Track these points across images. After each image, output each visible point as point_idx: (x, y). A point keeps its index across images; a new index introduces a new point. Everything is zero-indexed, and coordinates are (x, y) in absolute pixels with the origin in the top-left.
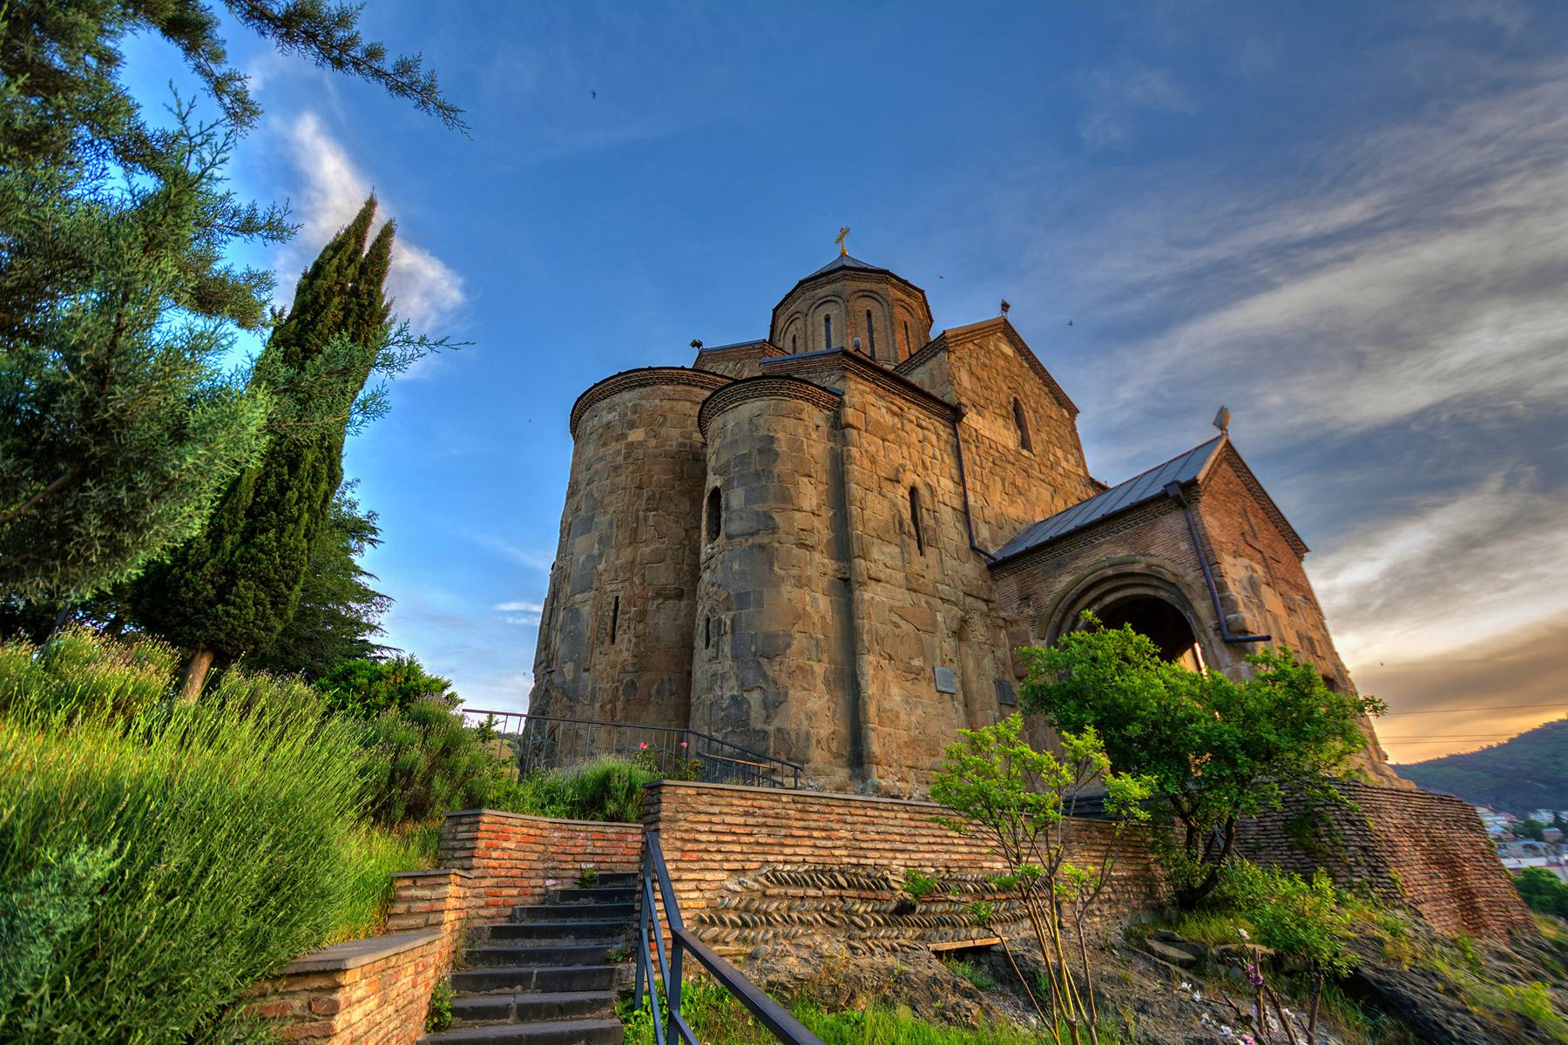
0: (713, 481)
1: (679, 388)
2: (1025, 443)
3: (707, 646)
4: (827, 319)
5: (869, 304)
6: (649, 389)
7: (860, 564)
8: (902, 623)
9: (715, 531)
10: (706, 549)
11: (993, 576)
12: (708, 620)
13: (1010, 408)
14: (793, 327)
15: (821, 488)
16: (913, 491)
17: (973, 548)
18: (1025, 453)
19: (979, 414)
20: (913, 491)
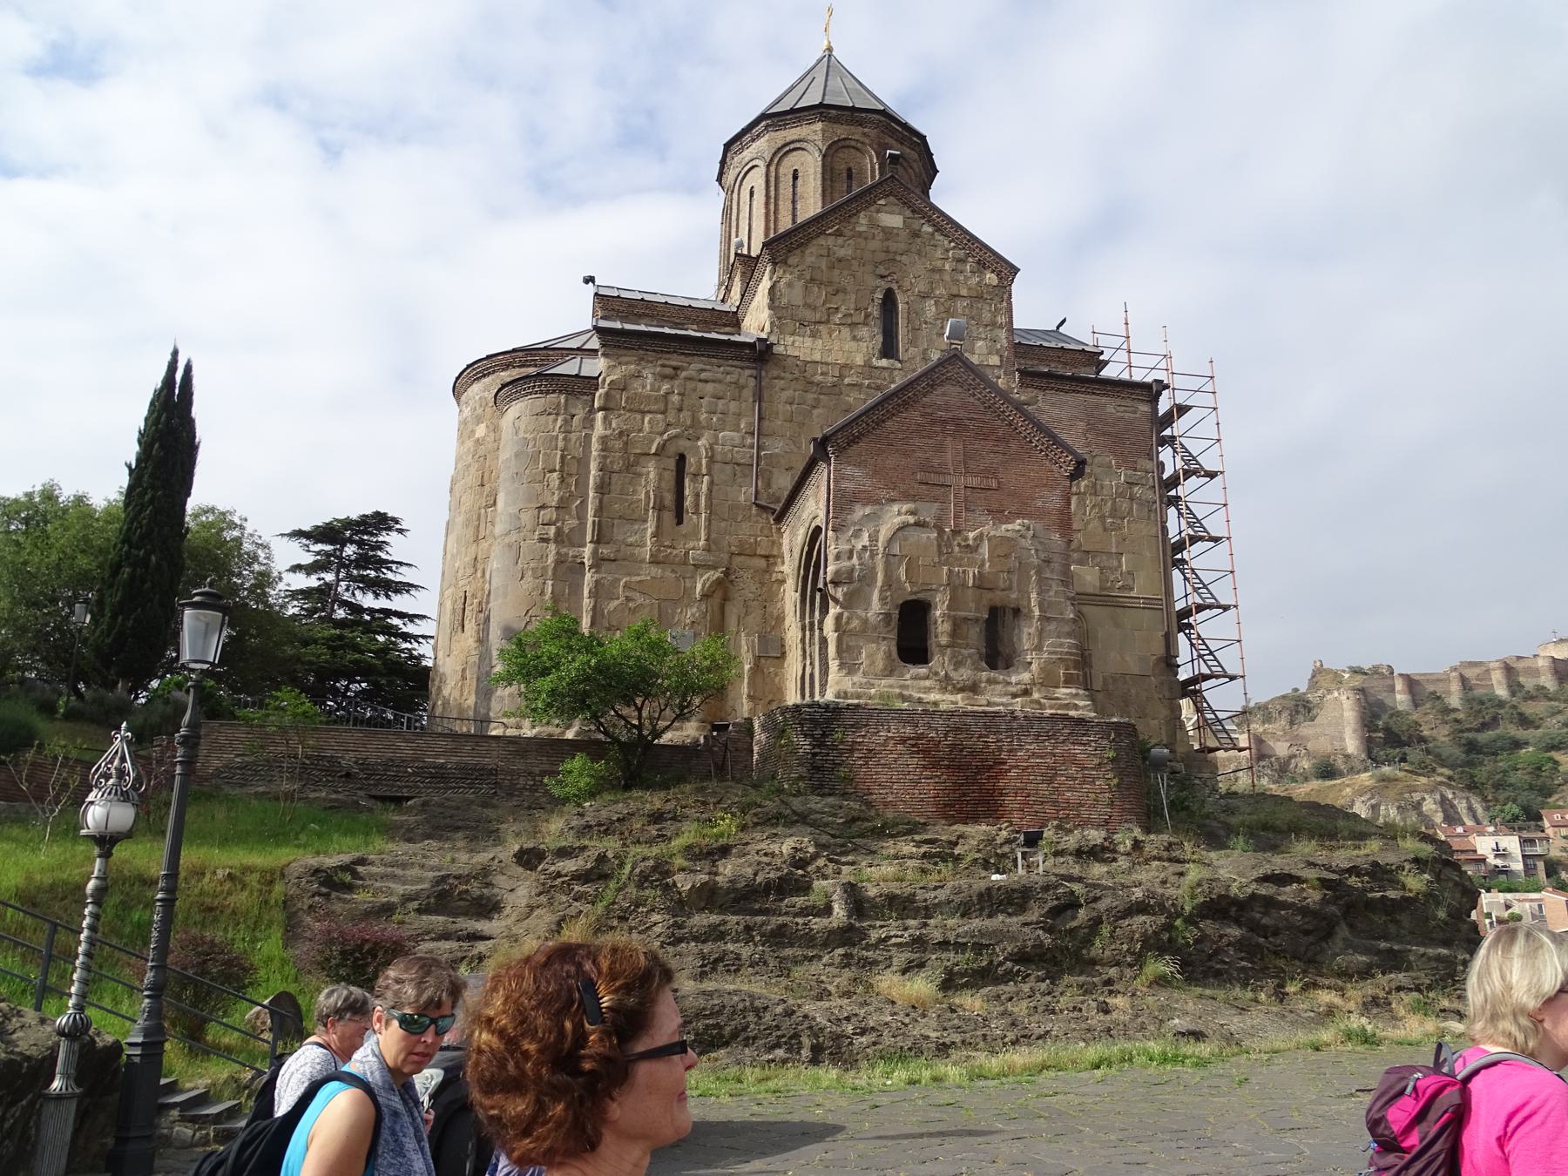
13: (875, 311)
18: (884, 362)
19: (814, 335)
20: (681, 459)
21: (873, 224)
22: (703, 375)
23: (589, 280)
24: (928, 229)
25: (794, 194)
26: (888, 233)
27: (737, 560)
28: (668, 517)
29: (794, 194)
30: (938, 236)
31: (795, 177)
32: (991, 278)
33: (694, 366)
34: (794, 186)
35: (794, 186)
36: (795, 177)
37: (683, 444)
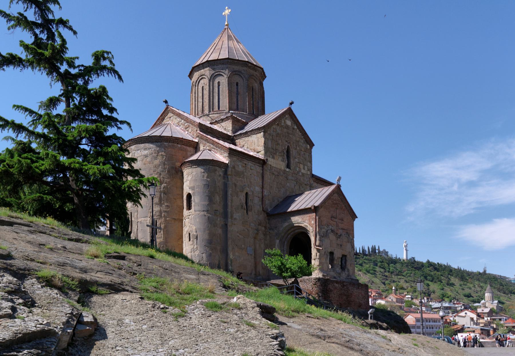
0: (187, 189)
1: (170, 144)
2: (288, 166)
3: (190, 240)
4: (219, 86)
5: (237, 79)
6: (159, 143)
7: (229, 220)
8: (240, 236)
9: (189, 207)
10: (186, 212)
11: (269, 220)
12: (190, 234)
13: (285, 152)
14: (202, 81)
15: (220, 196)
16: (247, 194)
17: (263, 210)
18: (288, 170)
19: (273, 158)
20: (247, 194)
21: (285, 122)
22: (252, 168)
23: (166, 102)
24: (296, 127)
25: (238, 91)
26: (287, 127)
27: (260, 227)
28: (245, 211)
29: (238, 91)
30: (298, 130)
31: (237, 84)
32: (308, 147)
33: (250, 164)
34: (237, 88)
35: (237, 88)
36: (237, 84)
37: (247, 189)
